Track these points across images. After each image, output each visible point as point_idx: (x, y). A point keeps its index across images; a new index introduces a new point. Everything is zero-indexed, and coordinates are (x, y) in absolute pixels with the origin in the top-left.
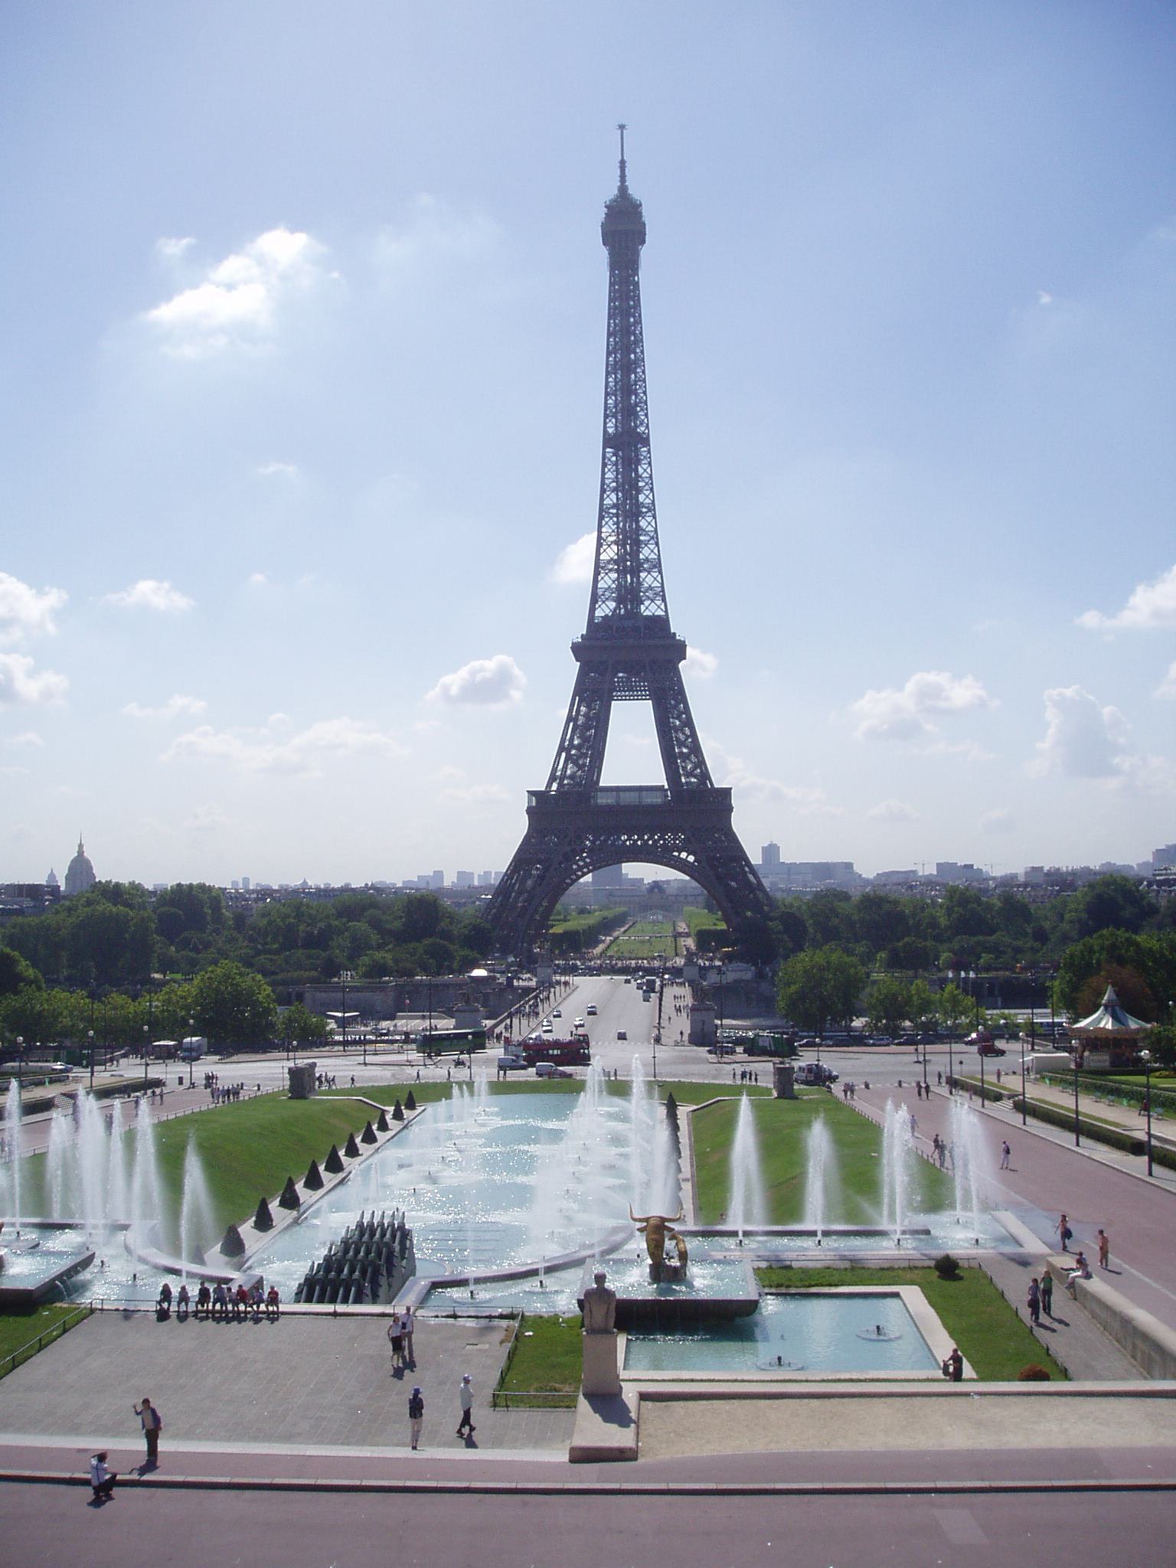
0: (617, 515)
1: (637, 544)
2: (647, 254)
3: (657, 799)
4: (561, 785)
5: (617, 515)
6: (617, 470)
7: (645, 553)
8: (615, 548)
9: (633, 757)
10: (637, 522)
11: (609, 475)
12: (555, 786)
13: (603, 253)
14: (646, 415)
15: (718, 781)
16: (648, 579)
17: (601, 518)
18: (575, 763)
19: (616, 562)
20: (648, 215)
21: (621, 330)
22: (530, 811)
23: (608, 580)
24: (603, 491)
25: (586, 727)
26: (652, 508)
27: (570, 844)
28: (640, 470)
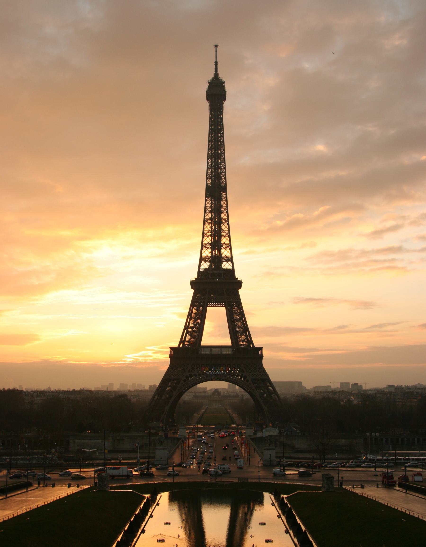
0: (211, 223)
1: (220, 237)
3: (228, 352)
4: (184, 345)
5: (211, 223)
6: (212, 203)
7: (224, 240)
8: (210, 238)
9: (216, 332)
10: (221, 227)
11: (208, 205)
12: (181, 345)
13: (206, 105)
14: (225, 178)
16: (225, 253)
17: (204, 224)
18: (191, 335)
19: (210, 244)
20: (227, 87)
21: (215, 139)
23: (207, 253)
24: (205, 212)
25: (195, 319)
28: (222, 203)
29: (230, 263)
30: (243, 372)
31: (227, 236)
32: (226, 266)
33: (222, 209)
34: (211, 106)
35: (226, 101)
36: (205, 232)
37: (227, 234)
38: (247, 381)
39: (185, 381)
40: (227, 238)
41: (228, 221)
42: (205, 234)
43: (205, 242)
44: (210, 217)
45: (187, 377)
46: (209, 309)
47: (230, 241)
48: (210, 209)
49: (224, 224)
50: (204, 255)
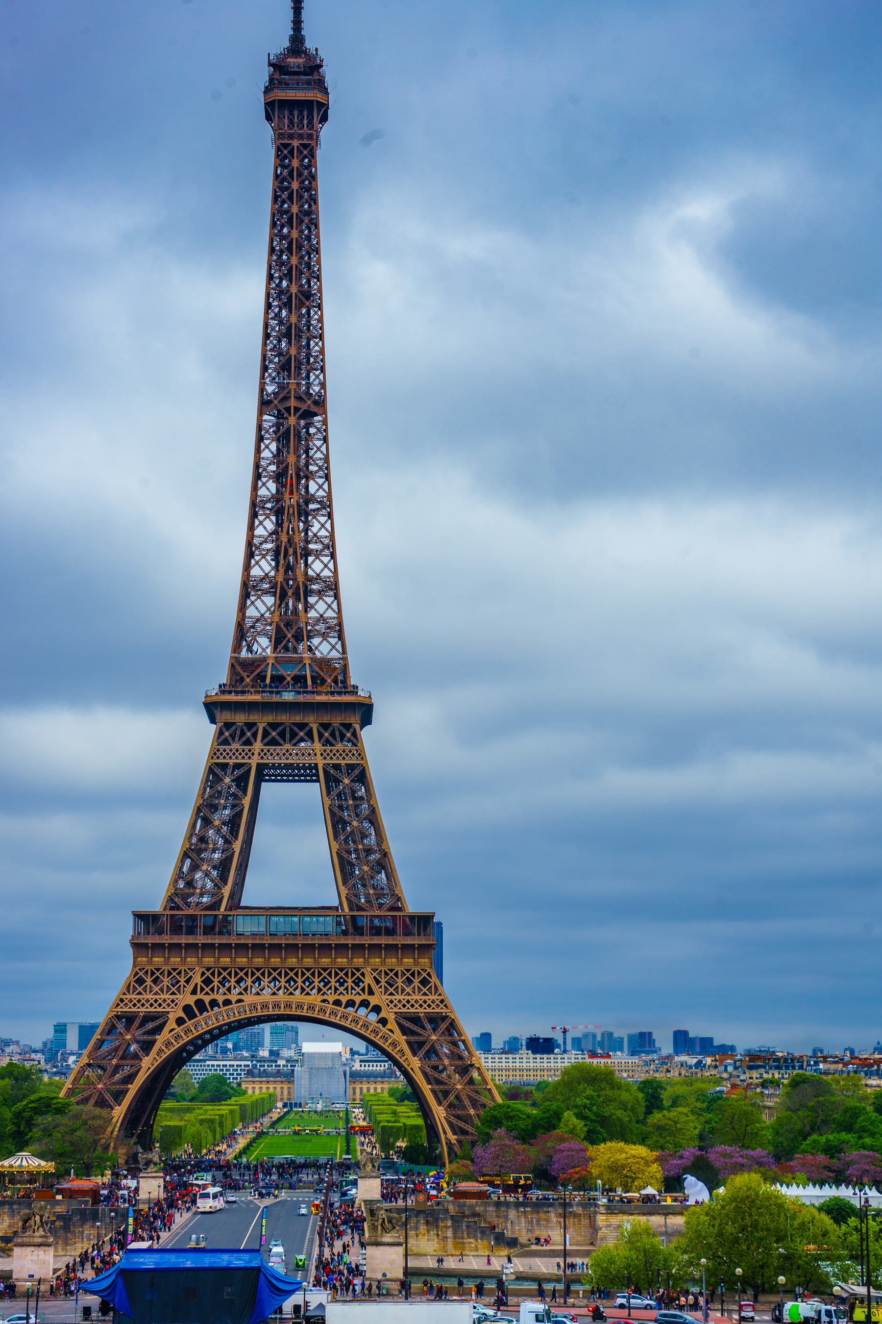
16: (320, 607)
17: (254, 515)
24: (257, 476)
26: (327, 505)
27: (194, 992)
29: (333, 641)
30: (371, 993)
31: (327, 552)
33: (313, 468)
34: (279, 135)
36: (256, 541)
37: (327, 547)
38: (383, 1022)
39: (180, 1021)
40: (326, 559)
41: (330, 506)
42: (257, 548)
43: (256, 572)
44: (274, 491)
45: (187, 1009)
47: (335, 572)
48: (273, 468)
50: (251, 612)
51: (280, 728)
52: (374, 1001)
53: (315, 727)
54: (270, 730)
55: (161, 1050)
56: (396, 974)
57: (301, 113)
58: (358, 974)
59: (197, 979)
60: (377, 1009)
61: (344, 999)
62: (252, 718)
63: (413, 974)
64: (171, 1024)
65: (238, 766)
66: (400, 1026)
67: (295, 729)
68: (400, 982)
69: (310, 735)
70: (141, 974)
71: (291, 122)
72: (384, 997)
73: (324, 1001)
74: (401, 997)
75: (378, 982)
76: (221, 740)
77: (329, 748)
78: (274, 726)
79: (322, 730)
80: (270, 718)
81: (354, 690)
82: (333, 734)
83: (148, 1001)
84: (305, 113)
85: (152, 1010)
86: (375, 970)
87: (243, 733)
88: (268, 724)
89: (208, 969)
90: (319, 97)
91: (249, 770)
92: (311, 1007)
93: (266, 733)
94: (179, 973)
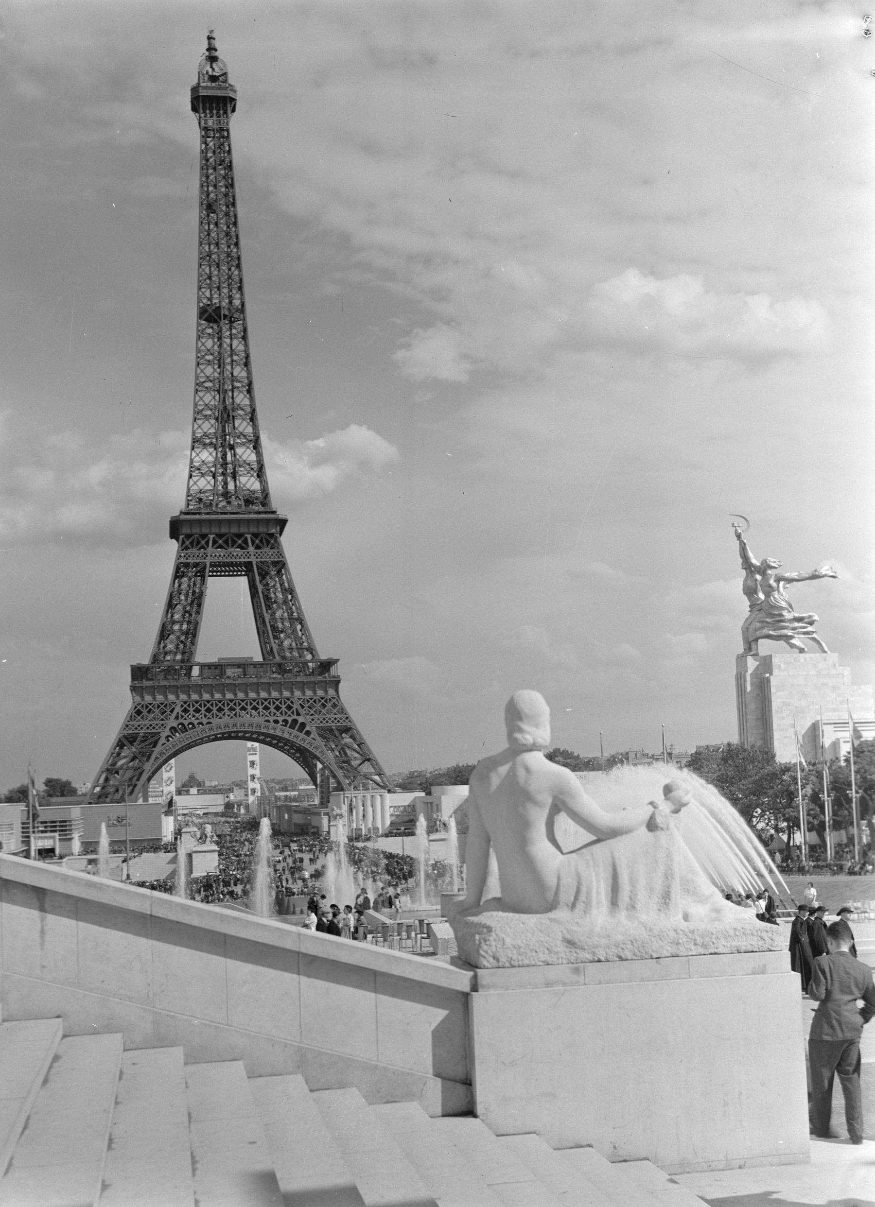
2: (236, 123)
7: (243, 426)
15: (323, 656)
22: (133, 689)
27: (177, 718)
30: (298, 714)
32: (249, 483)
35: (235, 114)
38: (308, 733)
46: (211, 581)
49: (241, 392)
51: (224, 539)
52: (301, 720)
53: (249, 536)
54: (217, 539)
55: (157, 758)
56: (315, 701)
57: (218, 106)
58: (289, 702)
59: (178, 709)
60: (303, 725)
61: (280, 719)
62: (205, 530)
63: (326, 701)
64: (163, 740)
65: (196, 565)
66: (320, 735)
67: (236, 539)
68: (318, 705)
69: (245, 541)
70: (139, 707)
71: (211, 112)
72: (308, 717)
73: (268, 721)
74: (320, 716)
75: (303, 707)
76: (184, 547)
77: (259, 551)
78: (220, 536)
79: (254, 539)
80: (215, 530)
81: (274, 512)
82: (261, 541)
83: (144, 725)
84: (221, 105)
85: (149, 731)
86: (300, 699)
87: (199, 542)
88: (217, 535)
89: (185, 703)
90: (231, 95)
91: (205, 567)
92: (259, 726)
93: (215, 542)
94: (165, 706)
